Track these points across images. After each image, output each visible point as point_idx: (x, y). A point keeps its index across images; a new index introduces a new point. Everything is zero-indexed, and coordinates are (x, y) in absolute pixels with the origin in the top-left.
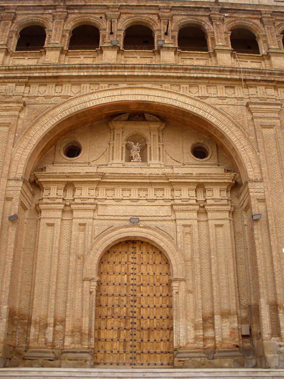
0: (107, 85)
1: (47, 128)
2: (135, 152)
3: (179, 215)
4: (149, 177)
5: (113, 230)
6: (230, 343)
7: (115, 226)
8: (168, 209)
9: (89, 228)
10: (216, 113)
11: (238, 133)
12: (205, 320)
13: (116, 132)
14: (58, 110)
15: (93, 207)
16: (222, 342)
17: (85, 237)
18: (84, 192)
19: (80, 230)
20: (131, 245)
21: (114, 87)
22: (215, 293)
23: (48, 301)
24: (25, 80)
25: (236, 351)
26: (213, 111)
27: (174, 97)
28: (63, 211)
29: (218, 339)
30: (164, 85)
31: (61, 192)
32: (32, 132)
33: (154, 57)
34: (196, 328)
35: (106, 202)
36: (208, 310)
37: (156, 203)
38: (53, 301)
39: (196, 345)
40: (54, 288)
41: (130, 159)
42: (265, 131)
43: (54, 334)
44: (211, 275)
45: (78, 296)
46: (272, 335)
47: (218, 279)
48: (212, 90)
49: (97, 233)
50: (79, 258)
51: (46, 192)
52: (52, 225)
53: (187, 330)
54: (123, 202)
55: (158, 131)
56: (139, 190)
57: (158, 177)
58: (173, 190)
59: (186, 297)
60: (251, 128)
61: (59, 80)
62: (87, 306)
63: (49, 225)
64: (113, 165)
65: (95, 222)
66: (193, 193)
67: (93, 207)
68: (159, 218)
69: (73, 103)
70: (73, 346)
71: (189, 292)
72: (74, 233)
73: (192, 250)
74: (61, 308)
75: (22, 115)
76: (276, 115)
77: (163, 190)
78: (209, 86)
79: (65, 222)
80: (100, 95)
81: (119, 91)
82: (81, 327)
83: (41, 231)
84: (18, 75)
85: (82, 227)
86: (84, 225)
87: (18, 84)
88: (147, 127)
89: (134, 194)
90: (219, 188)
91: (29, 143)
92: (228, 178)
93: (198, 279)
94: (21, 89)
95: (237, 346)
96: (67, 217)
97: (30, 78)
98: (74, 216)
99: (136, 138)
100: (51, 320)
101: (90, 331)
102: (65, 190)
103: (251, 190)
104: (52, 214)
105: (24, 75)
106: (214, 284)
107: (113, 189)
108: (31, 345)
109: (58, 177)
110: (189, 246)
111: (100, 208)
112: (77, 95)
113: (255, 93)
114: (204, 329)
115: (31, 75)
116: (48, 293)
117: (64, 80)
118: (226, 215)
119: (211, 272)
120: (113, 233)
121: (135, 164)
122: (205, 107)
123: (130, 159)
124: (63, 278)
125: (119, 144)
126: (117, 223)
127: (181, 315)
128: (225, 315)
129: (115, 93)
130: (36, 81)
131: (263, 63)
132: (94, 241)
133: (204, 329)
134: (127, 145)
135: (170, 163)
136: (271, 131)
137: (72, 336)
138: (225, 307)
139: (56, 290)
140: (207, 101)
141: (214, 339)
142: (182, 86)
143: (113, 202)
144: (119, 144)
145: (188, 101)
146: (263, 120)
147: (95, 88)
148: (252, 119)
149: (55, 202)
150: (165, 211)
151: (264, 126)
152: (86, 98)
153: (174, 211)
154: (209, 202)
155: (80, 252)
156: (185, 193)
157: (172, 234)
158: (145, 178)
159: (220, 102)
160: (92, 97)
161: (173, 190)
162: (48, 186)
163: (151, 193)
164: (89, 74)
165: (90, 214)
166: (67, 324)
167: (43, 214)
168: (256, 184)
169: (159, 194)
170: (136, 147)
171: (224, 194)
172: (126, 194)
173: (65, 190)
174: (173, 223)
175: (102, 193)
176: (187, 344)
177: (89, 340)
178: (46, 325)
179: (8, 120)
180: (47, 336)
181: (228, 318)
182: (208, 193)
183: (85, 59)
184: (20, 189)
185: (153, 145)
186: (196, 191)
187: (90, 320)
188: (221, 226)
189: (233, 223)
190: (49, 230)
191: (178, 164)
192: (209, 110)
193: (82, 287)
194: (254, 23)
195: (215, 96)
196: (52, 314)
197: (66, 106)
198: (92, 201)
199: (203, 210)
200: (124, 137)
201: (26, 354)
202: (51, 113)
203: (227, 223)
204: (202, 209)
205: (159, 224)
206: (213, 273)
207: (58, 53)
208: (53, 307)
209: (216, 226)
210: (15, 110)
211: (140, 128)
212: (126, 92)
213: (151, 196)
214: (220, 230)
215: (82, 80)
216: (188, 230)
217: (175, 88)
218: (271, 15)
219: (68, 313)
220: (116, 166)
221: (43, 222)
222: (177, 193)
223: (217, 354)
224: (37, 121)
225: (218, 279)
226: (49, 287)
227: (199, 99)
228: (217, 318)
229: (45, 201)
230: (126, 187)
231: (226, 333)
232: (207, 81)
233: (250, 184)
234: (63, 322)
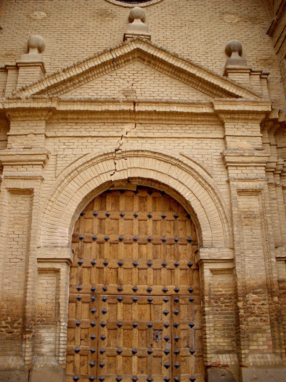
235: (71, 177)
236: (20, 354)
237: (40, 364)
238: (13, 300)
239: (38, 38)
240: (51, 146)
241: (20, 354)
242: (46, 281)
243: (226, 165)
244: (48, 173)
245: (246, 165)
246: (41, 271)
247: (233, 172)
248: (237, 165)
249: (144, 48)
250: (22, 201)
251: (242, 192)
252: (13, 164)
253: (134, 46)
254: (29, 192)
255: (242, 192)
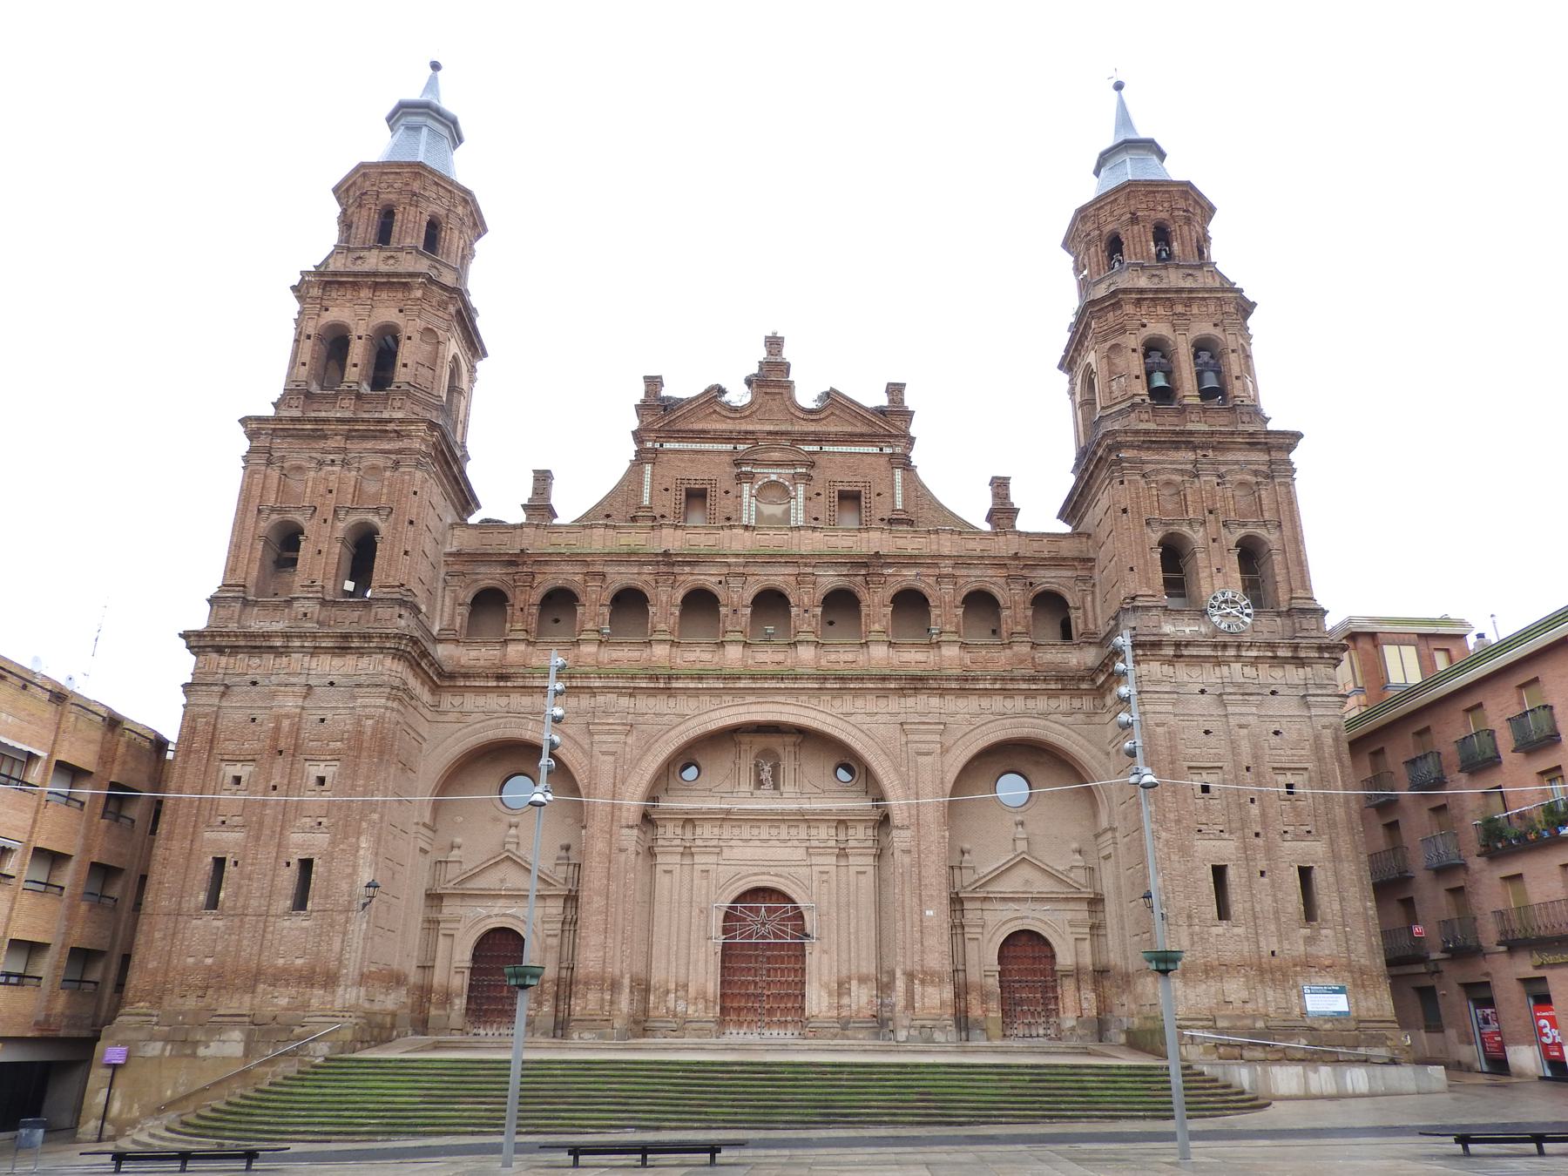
0: (731, 698)
1: (661, 758)
2: (766, 775)
3: (816, 860)
4: (782, 814)
5: (740, 879)
6: (867, 1012)
7: (743, 874)
8: (803, 851)
9: (713, 875)
10: (862, 735)
11: (887, 764)
12: (840, 985)
13: (743, 747)
14: (672, 733)
15: (717, 850)
16: (858, 1011)
17: (708, 887)
18: (706, 831)
19: (702, 878)
20: (761, 894)
21: (740, 701)
22: (852, 955)
23: (669, 962)
24: (629, 691)
25: (873, 1022)
26: (859, 734)
27: (813, 714)
28: (682, 854)
29: (854, 1007)
30: (801, 698)
31: (679, 831)
32: (644, 764)
33: (789, 651)
34: (830, 994)
35: (732, 843)
36: (844, 973)
37: (789, 844)
38: (674, 964)
39: (829, 1014)
40: (675, 948)
41: (759, 783)
42: (921, 759)
43: (676, 1001)
44: (849, 933)
45: (702, 956)
46: (906, 1008)
47: (857, 938)
48: (860, 703)
49: (722, 881)
50: (701, 912)
51: (661, 830)
52: (671, 872)
53: (820, 997)
54: (751, 843)
55: (794, 745)
56: (770, 827)
57: (791, 813)
58: (809, 827)
59: (820, 958)
60: (904, 755)
61: (673, 691)
62: (711, 968)
63: (665, 871)
64: (741, 795)
65: (720, 868)
66: (833, 832)
67: (717, 850)
68: (793, 863)
69: (691, 724)
70: (697, 1014)
71: (825, 952)
72: (695, 882)
73: (829, 902)
74: (682, 971)
75: (629, 740)
76: (937, 738)
77: (798, 826)
78: (857, 697)
79: (685, 867)
80: (723, 713)
81: (746, 707)
82: (705, 993)
83: (657, 880)
84: (621, 685)
85: (705, 874)
86: (708, 871)
87: (620, 695)
88: (780, 740)
89: (765, 832)
90: (864, 825)
91: (641, 779)
92: (876, 815)
93: (834, 936)
94: (624, 702)
95: (874, 1016)
96: (687, 861)
97: (635, 688)
98: (696, 861)
99: (767, 754)
100: (672, 986)
101: (715, 997)
102: (683, 827)
103: (895, 839)
104: (669, 859)
105: (627, 685)
106: (852, 944)
107: (740, 827)
108: (651, 1014)
109: (674, 814)
110: (826, 897)
111: (725, 849)
112: (696, 712)
113: (914, 705)
114: (839, 995)
115: (637, 685)
116: (668, 954)
117: (678, 691)
118: (870, 860)
119: (849, 928)
120: (741, 883)
121: (765, 792)
122: (850, 728)
123: (759, 783)
124: (684, 935)
125: (747, 762)
126: (744, 870)
127: (814, 979)
128: (862, 980)
129: (742, 709)
130: (643, 691)
131: (932, 653)
132: (719, 892)
133: (839, 995)
134: (756, 765)
135: (808, 788)
136: (929, 759)
137: (695, 1004)
138: (864, 970)
139: (677, 951)
140: (852, 719)
141: (850, 1006)
142: (822, 698)
143: (741, 844)
144: (747, 762)
145: (829, 720)
146: (919, 745)
147: (716, 701)
148: (907, 743)
149: (673, 843)
150: (800, 854)
151: (919, 754)
152: (705, 717)
153: (809, 855)
154: (852, 843)
155: (703, 905)
156: (824, 832)
157: (806, 882)
158: (777, 814)
159: (869, 719)
160: (713, 715)
161: (809, 827)
162: (663, 822)
163: (784, 832)
164: (709, 686)
165: (713, 859)
166: (690, 990)
167: (660, 859)
168: (902, 831)
169: (793, 831)
170: (767, 768)
171: (870, 832)
172: (755, 831)
173: (683, 827)
174: (808, 869)
175: (727, 832)
176: (820, 1012)
177: (714, 1007)
178: (668, 992)
179: (613, 748)
180: (669, 1005)
181: (866, 983)
182: (851, 832)
183: (702, 654)
184: (635, 838)
185: (788, 764)
186: (836, 828)
187: (715, 985)
188: (865, 873)
189: (878, 868)
190: (667, 877)
191: (819, 791)
192: (855, 731)
193: (706, 946)
194: (926, 585)
195: (863, 711)
196: (674, 979)
197: (682, 728)
198: (715, 843)
199: (843, 853)
200: (753, 755)
201: (647, 1024)
202: (665, 738)
203: (870, 870)
204: (842, 851)
205: (792, 870)
206: (852, 930)
207: (668, 647)
208: (674, 970)
209: (858, 872)
210: (620, 733)
211: (773, 742)
212: (754, 708)
213: (784, 836)
214: (861, 877)
215: (700, 692)
216: (825, 877)
217: (814, 701)
218: (953, 568)
219: (690, 978)
220: (743, 795)
221: (659, 869)
222: (813, 832)
223: (852, 1025)
224: (649, 749)
225: (857, 938)
226: (669, 948)
227: (842, 716)
228: (854, 983)
229: (660, 842)
230: (755, 824)
231: (864, 1000)
232: (853, 692)
233: (895, 832)
234: (686, 986)
235: (472, 927)
236: (445, 1009)
237: (453, 1015)
238: (442, 986)
239: (458, 840)
240: (461, 911)
241: (445, 1009)
242: (459, 977)
243: (544, 922)
244: (460, 926)
245: (553, 922)
246: (456, 972)
247: (546, 926)
248: (548, 922)
249: (511, 855)
250: (449, 940)
251: (548, 936)
252: (444, 921)
253: (507, 854)
254: (453, 935)
255: (548, 936)
